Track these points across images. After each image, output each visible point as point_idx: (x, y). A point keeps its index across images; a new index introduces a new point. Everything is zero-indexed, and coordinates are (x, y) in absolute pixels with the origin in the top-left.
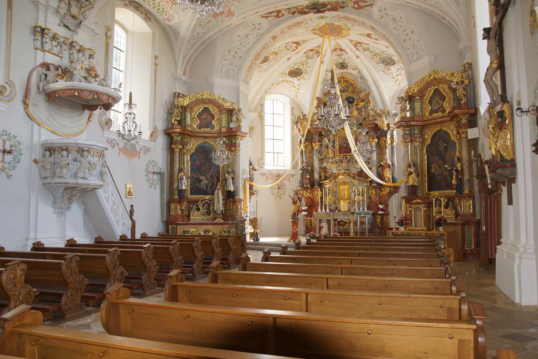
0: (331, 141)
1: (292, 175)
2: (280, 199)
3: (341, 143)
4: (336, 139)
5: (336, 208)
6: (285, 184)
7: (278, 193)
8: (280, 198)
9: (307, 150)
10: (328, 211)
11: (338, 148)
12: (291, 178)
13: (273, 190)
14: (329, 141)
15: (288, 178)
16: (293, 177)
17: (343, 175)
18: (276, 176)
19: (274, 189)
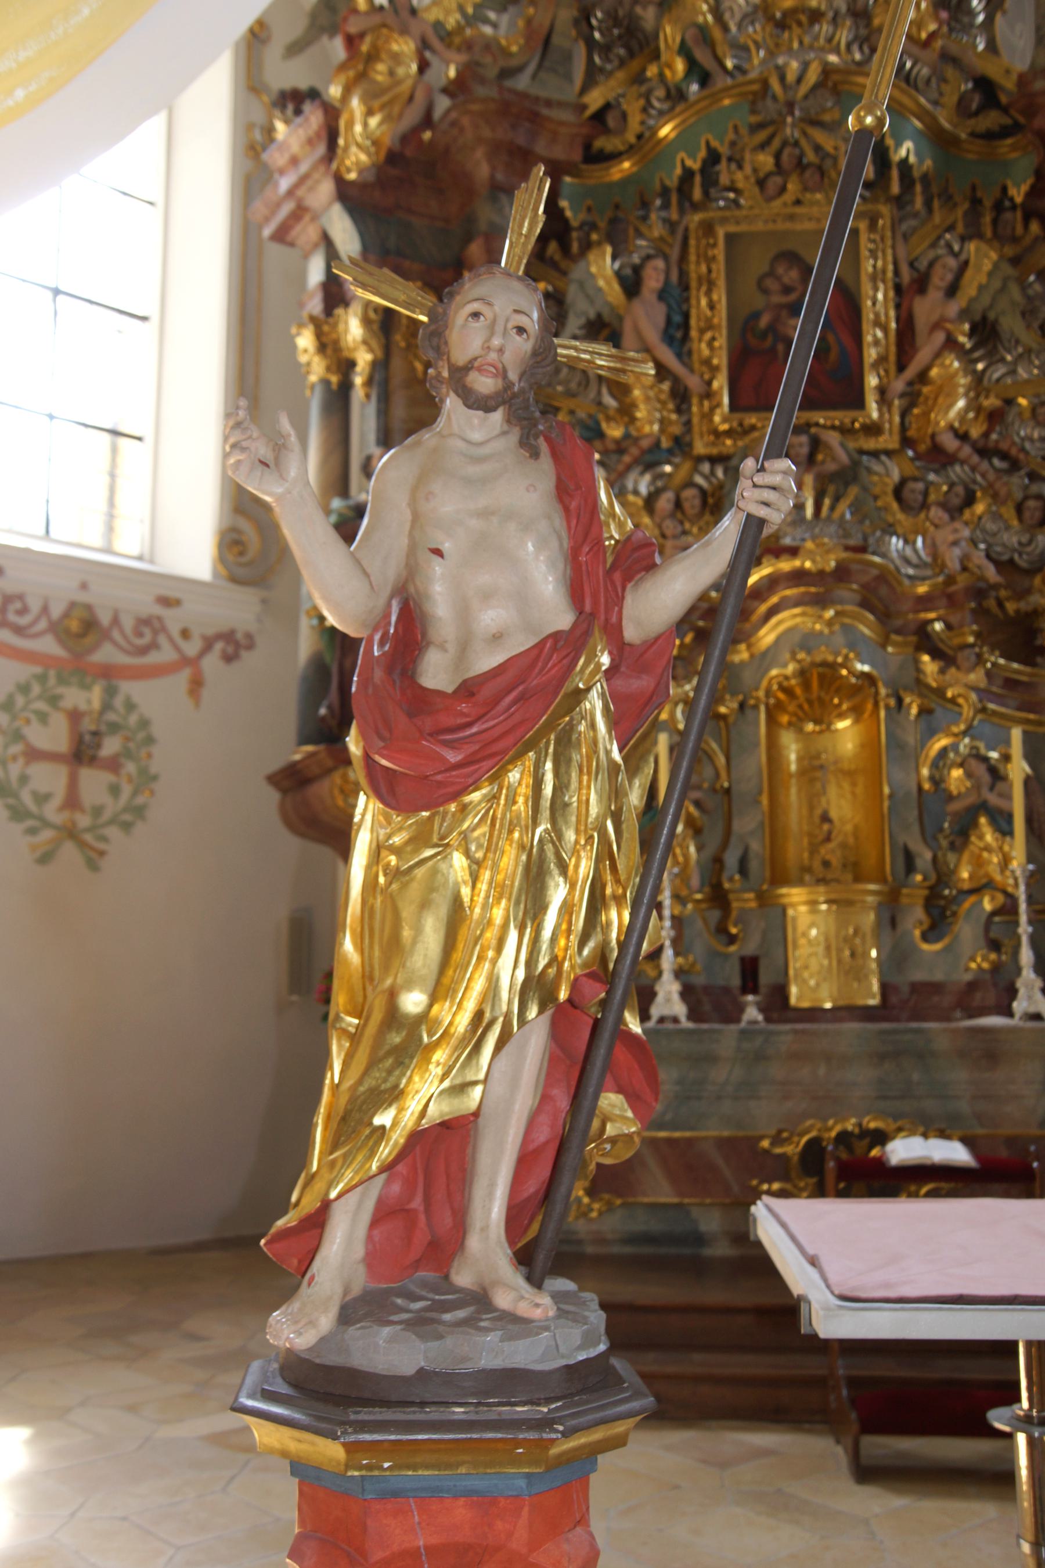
0: (653, 279)
1: (228, 637)
2: (93, 866)
3: (759, 301)
4: (696, 269)
5: (750, 968)
6: (144, 723)
7: (72, 801)
8: (94, 859)
9: (397, 364)
10: (679, 1009)
11: (721, 360)
12: (211, 664)
13: (15, 769)
14: (631, 285)
15: (192, 662)
16: (229, 658)
17: (820, 601)
18: (58, 629)
19: (34, 755)
